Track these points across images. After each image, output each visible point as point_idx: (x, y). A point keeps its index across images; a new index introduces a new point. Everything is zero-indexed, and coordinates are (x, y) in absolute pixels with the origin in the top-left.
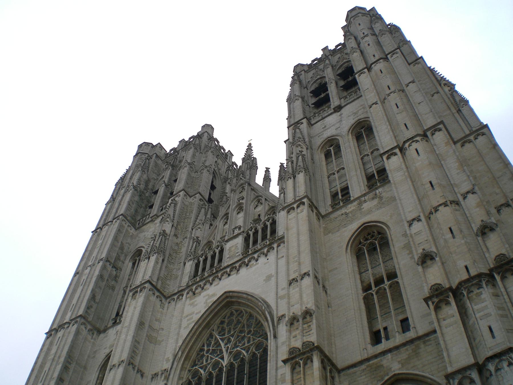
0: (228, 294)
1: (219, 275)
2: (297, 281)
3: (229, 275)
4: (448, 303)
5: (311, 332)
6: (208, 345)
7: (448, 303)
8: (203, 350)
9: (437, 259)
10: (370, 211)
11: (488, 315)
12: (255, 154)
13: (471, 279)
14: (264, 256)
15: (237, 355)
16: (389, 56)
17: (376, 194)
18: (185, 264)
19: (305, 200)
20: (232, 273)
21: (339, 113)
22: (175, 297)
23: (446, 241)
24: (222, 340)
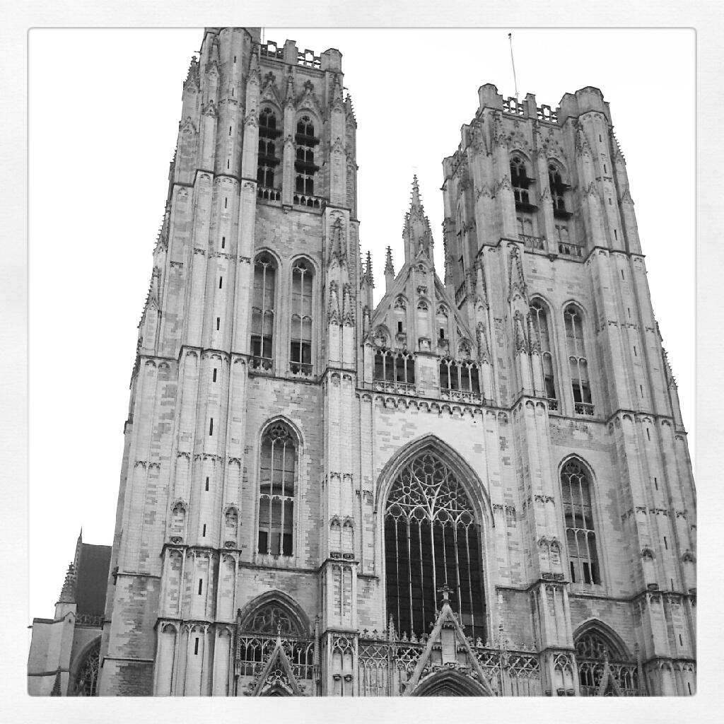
0: (434, 439)
1: (419, 402)
2: (543, 501)
3: (429, 411)
4: (658, 602)
5: (559, 563)
7: (658, 602)
9: (655, 560)
10: (579, 444)
11: (680, 627)
13: (674, 594)
14: (470, 415)
15: (442, 516)
16: (634, 257)
18: (363, 346)
19: (545, 403)
20: (433, 410)
22: (361, 394)
23: (660, 547)
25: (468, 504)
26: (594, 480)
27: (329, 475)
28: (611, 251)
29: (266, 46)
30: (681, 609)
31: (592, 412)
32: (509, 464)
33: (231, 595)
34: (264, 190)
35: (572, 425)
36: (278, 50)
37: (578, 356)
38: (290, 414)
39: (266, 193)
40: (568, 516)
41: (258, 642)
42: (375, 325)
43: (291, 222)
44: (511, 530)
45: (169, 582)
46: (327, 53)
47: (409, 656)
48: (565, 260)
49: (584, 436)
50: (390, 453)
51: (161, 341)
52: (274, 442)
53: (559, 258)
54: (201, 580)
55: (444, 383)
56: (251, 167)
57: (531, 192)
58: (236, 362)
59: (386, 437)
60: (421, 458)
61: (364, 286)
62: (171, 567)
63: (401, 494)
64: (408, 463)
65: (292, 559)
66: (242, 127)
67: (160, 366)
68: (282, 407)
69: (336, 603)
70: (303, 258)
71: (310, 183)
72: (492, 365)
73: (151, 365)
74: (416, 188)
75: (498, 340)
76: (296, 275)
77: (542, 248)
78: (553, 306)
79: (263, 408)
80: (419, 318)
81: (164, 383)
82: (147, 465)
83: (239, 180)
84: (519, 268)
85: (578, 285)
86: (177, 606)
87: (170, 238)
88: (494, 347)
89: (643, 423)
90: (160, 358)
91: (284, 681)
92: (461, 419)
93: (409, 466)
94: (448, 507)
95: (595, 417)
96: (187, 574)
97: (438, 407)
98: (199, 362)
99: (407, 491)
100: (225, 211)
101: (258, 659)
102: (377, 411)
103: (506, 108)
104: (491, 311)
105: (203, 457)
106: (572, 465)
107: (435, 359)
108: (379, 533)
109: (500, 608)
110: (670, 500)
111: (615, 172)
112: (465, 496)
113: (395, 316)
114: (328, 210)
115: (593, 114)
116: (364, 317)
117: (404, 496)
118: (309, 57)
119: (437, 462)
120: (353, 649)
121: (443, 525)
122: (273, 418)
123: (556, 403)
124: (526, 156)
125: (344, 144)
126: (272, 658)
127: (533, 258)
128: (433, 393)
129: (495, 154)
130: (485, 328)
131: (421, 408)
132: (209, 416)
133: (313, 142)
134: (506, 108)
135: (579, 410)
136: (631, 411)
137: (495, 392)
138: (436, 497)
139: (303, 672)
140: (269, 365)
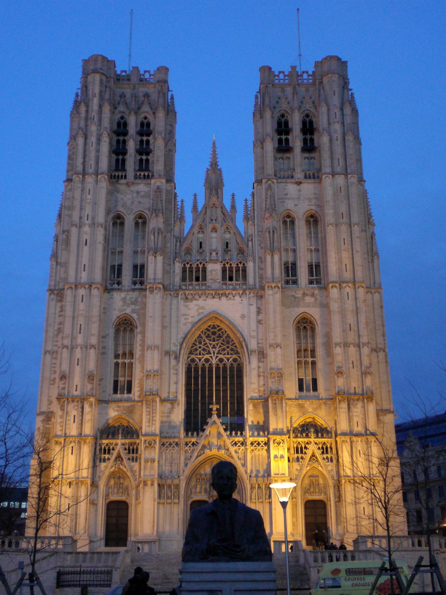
2: (274, 347)
3: (214, 297)
6: (200, 343)
8: (196, 345)
9: (344, 376)
10: (308, 306)
12: (221, 165)
15: (221, 360)
16: (349, 176)
17: (314, 293)
19: (280, 285)
20: (216, 297)
21: (298, 187)
22: (172, 293)
23: (349, 367)
24: (211, 344)
25: (237, 351)
26: (316, 327)
27: (146, 348)
28: (334, 174)
29: (119, 75)
30: (360, 404)
31: (320, 282)
32: (262, 324)
33: (90, 422)
34: (117, 174)
35: (304, 294)
36: (128, 75)
37: (313, 248)
38: (130, 311)
39: (118, 176)
40: (299, 351)
41: (109, 444)
42: (183, 248)
43: (132, 191)
44: (261, 364)
45: (58, 418)
46: (158, 69)
47: (191, 446)
48: (309, 183)
49: (312, 300)
50: (190, 326)
51: (58, 280)
52: (122, 329)
53: (304, 183)
54: (75, 416)
55: (224, 278)
56: (104, 164)
57: (290, 137)
58: (94, 289)
59: (187, 317)
60: (209, 326)
61: (178, 223)
62: (59, 410)
63: (196, 350)
64: (201, 330)
65: (131, 395)
66: (99, 140)
67: (58, 294)
68: (125, 308)
69: (147, 420)
70: (141, 213)
71: (147, 160)
72: (254, 262)
73: (52, 294)
74: (214, 151)
75: (260, 245)
76: (137, 224)
77: (292, 177)
78: (297, 217)
79: (115, 310)
80: (212, 238)
81: (59, 305)
82: (51, 352)
83: (97, 174)
84: (273, 196)
85: (316, 198)
86: (62, 430)
87: (62, 217)
88: (256, 250)
89: (345, 289)
90: (57, 290)
91: (122, 464)
92: (234, 300)
93: (202, 332)
94: (225, 354)
95: (321, 286)
96: (67, 413)
97: (219, 294)
98: (74, 292)
99: (200, 347)
100: (89, 197)
101: (109, 453)
102: (182, 302)
103: (277, 79)
104: (256, 226)
105: (75, 347)
106: (304, 318)
107: (219, 264)
108: (181, 376)
109: (250, 412)
110: (359, 336)
111: (343, 115)
112: (236, 347)
113: (198, 238)
114: (153, 181)
115: (329, 76)
116: (176, 244)
117: (198, 352)
118: (147, 76)
119: (219, 328)
120: (155, 446)
121: (221, 366)
122: (121, 315)
123: (297, 280)
124: (287, 112)
125: (163, 135)
126: (115, 453)
127: (285, 186)
128: (215, 286)
129: (264, 117)
130: (252, 239)
131: (209, 296)
132: (79, 323)
133: (148, 135)
134: (277, 79)
135: (311, 282)
136: (336, 282)
137: (255, 279)
138: (217, 349)
139: (133, 459)
140: (119, 283)
